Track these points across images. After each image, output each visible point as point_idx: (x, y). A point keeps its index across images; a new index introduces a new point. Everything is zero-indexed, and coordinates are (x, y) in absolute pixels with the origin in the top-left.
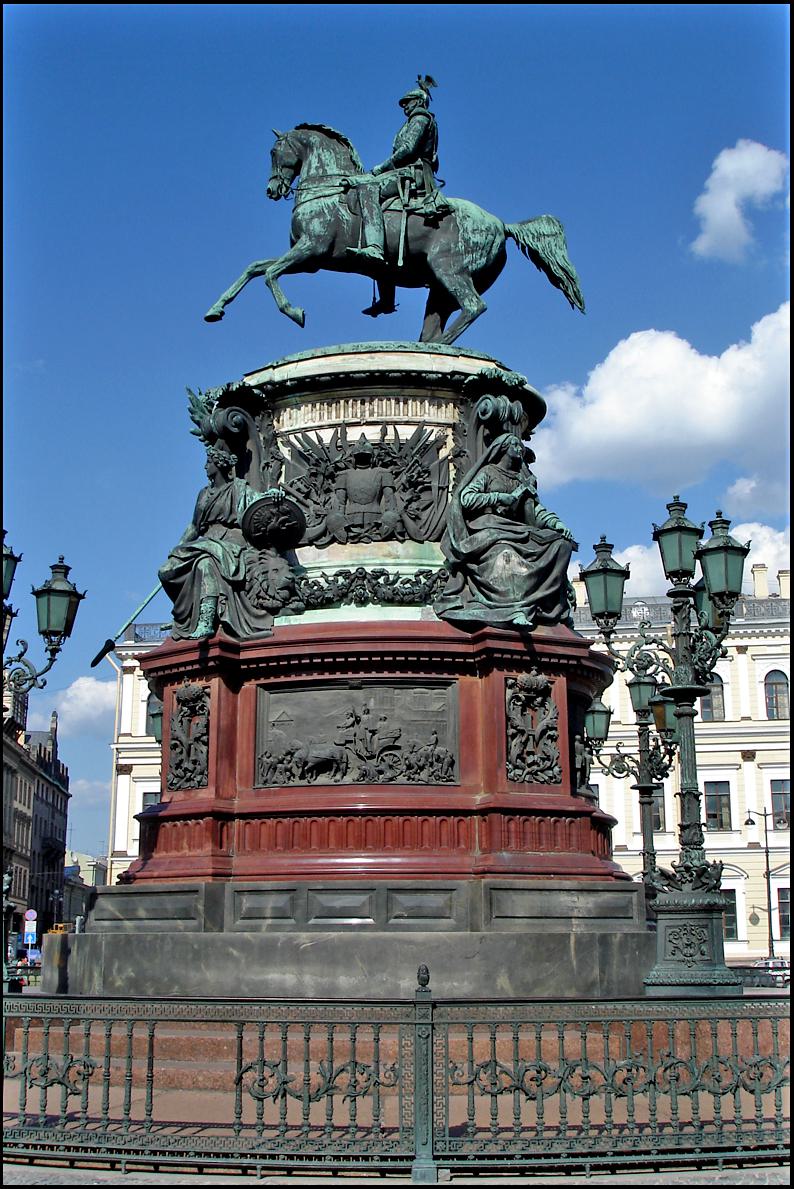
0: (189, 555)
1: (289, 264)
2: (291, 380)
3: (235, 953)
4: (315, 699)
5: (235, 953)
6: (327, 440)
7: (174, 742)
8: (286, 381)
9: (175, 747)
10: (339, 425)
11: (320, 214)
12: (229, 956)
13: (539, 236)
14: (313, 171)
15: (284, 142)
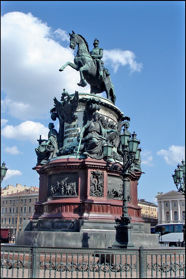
0: (100, 139)
1: (85, 69)
2: (104, 103)
3: (138, 238)
4: (116, 180)
5: (138, 238)
6: (105, 119)
7: (92, 184)
8: (103, 102)
9: (92, 185)
10: (108, 117)
11: (90, 61)
12: (137, 239)
13: (113, 87)
14: (84, 49)
15: (76, 36)
